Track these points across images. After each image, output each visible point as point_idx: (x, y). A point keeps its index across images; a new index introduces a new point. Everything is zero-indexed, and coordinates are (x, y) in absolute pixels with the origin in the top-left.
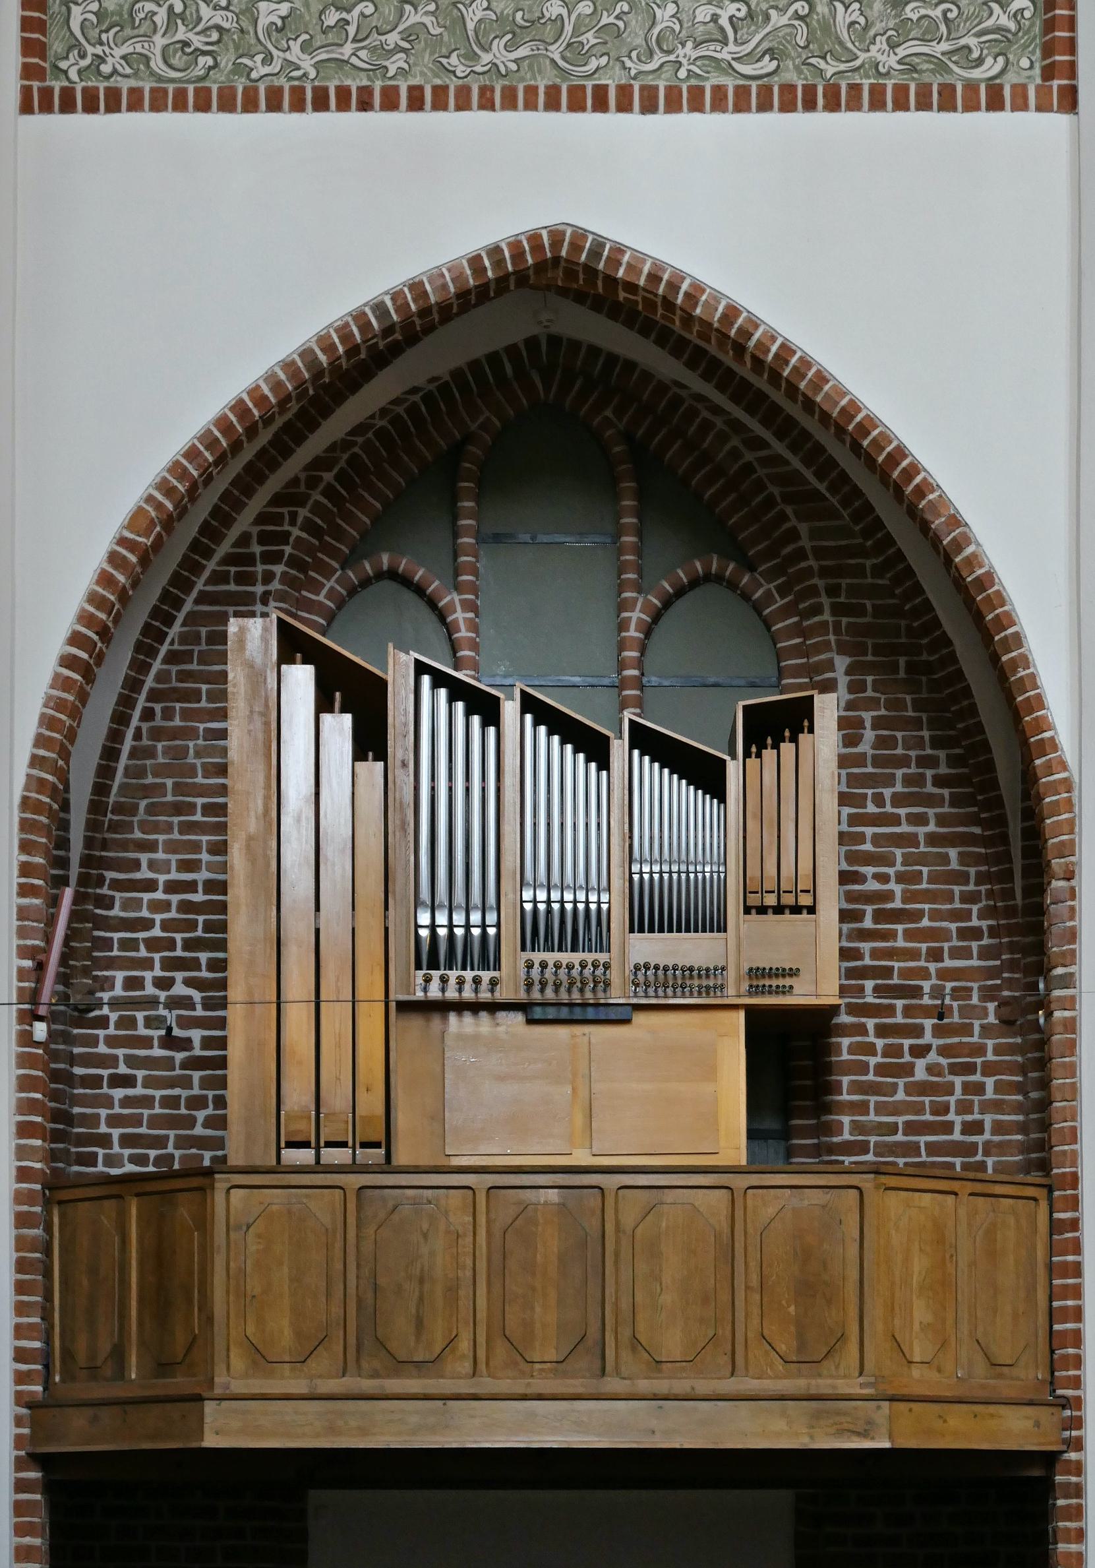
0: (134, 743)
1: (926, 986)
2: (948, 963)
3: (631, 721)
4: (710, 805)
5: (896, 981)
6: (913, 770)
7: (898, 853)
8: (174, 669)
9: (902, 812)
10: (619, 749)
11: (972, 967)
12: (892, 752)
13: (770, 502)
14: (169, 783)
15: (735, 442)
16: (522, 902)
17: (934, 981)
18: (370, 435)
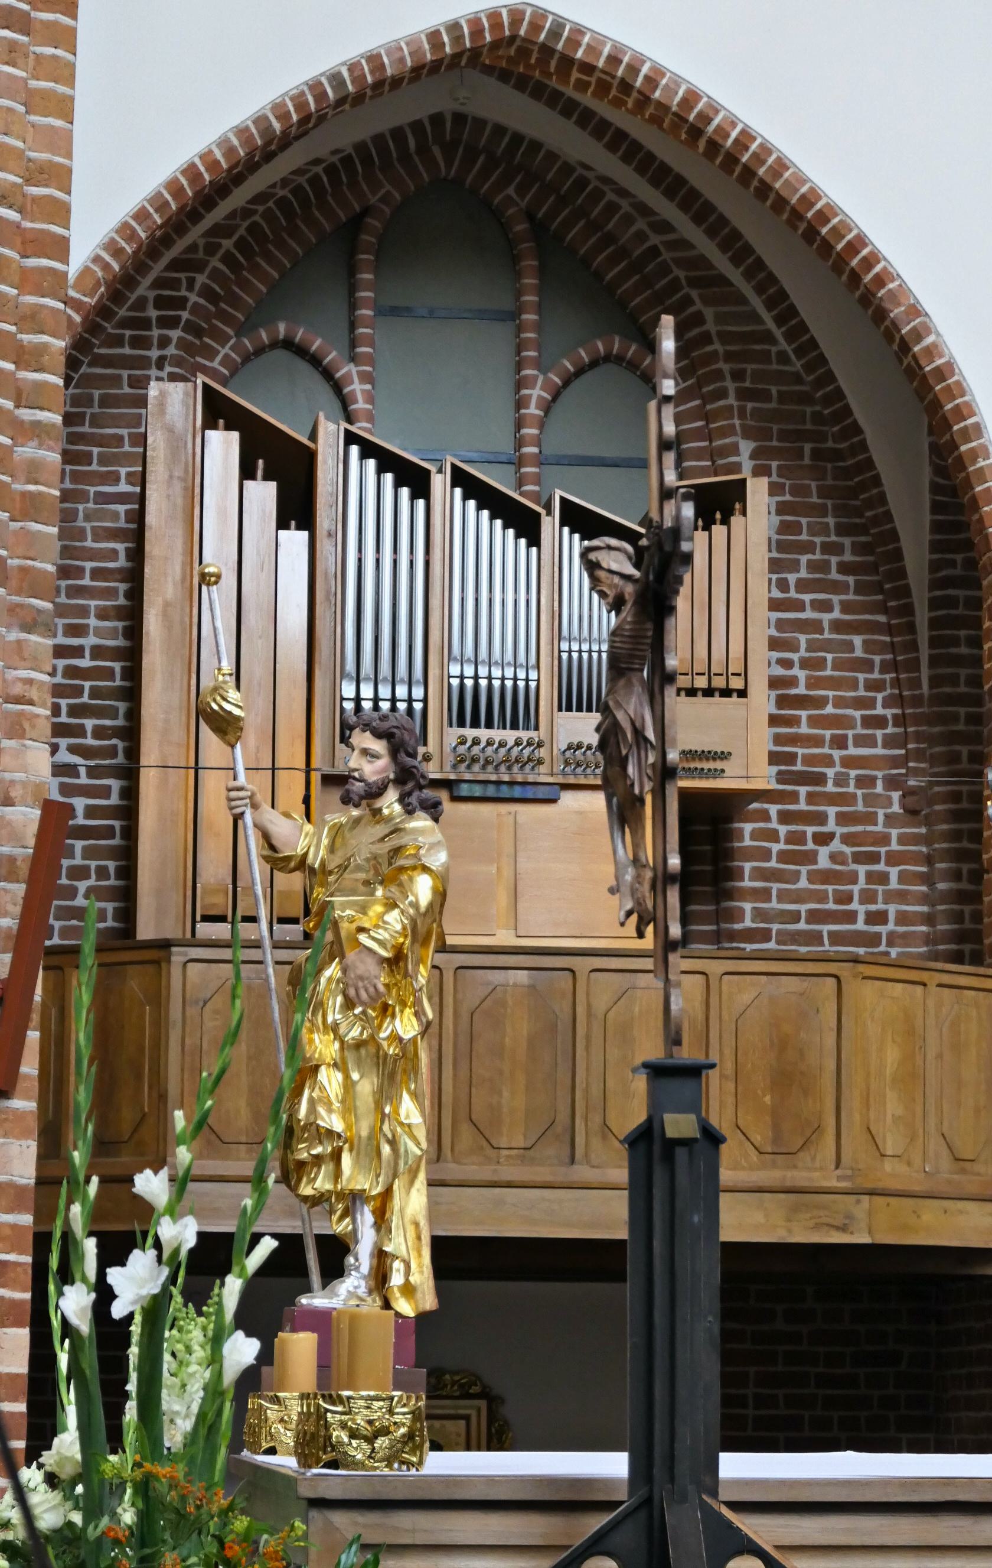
1: (830, 772)
2: (852, 751)
5: (799, 767)
6: (818, 556)
7: (803, 639)
9: (807, 598)
15: (641, 224)
17: (838, 768)
18: (271, 204)
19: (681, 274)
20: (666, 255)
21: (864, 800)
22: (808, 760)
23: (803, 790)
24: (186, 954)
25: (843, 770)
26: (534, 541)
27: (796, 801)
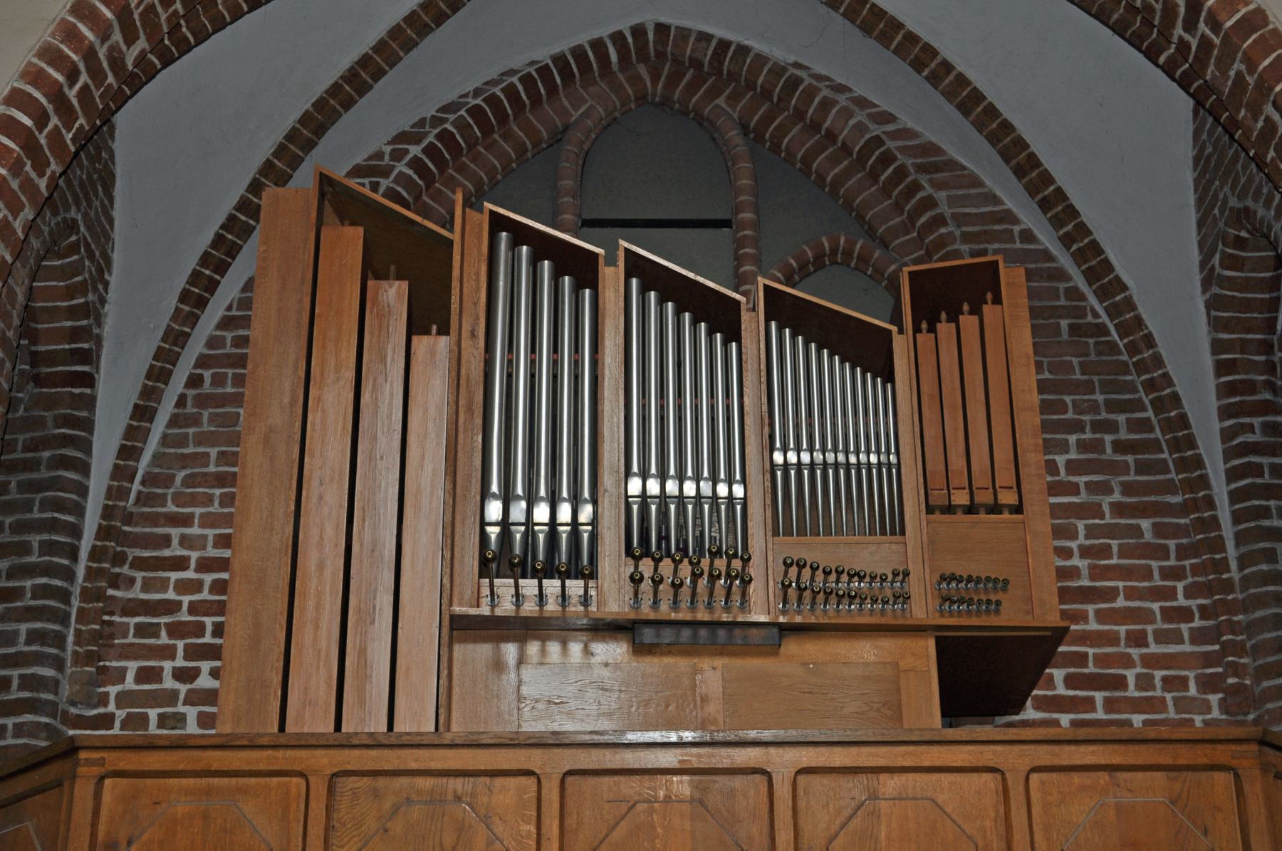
0: (176, 411)
1: (1130, 675)
2: (1153, 648)
3: (766, 286)
4: (872, 386)
5: (1091, 669)
6: (1088, 435)
7: (1081, 525)
8: (229, 336)
9: (1082, 480)
10: (752, 322)
11: (1184, 653)
12: (1062, 417)
13: (901, 173)
14: (213, 452)
15: (860, 117)
16: (627, 497)
17: (1139, 670)
18: (462, 112)
19: (909, 162)
20: (891, 144)
21: (1175, 705)
22: (1101, 660)
23: (1099, 696)
24: (101, 763)
25: (1145, 671)
26: (733, 334)
27: (1093, 709)
